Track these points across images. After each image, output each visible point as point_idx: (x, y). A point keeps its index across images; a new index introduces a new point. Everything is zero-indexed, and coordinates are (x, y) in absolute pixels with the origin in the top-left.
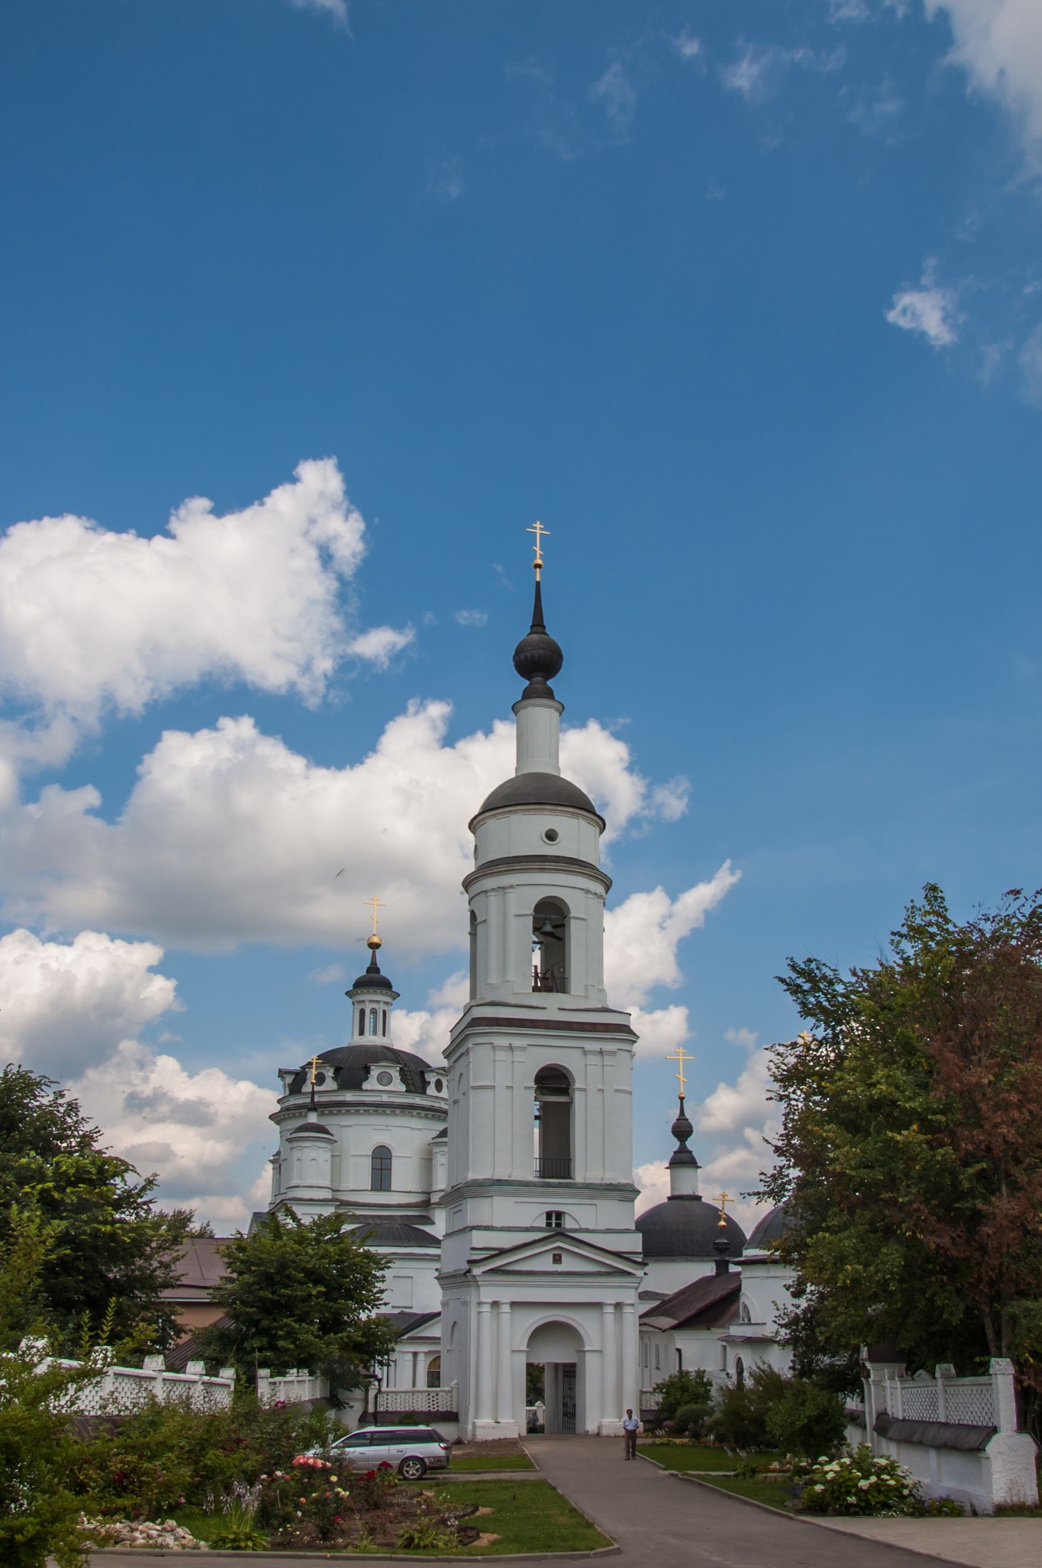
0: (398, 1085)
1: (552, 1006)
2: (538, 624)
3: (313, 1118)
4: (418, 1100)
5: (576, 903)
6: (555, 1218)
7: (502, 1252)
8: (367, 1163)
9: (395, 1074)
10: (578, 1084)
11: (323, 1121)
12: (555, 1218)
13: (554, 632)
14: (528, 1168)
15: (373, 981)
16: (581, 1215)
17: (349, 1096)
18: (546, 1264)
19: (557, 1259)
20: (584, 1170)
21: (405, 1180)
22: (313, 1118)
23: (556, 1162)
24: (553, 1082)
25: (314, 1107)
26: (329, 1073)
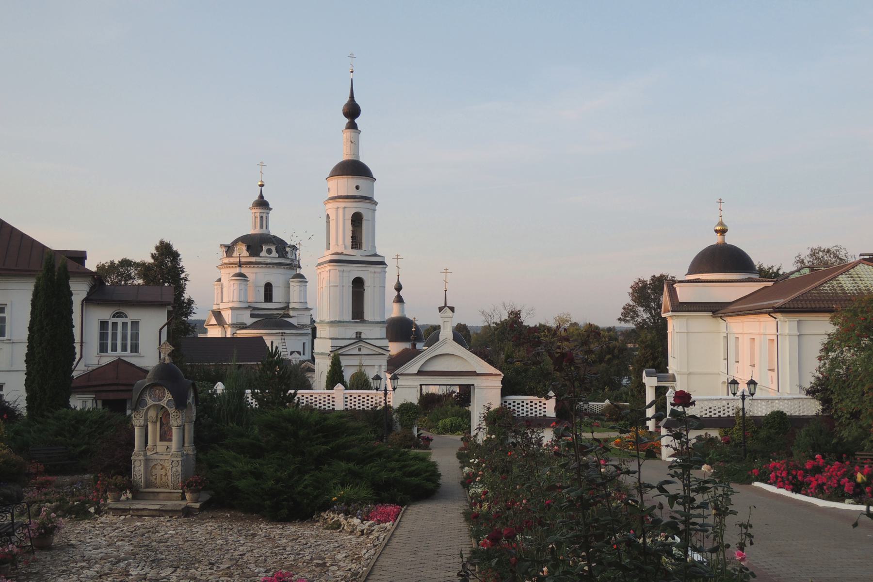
0: (274, 254)
1: (357, 255)
2: (352, 96)
3: (237, 270)
4: (283, 261)
5: (366, 216)
6: (359, 334)
7: (342, 347)
8: (263, 289)
9: (273, 248)
10: (366, 284)
11: (244, 270)
12: (359, 334)
13: (357, 100)
14: (348, 316)
15: (262, 204)
16: (368, 332)
17: (253, 259)
18: (356, 352)
19: (360, 350)
20: (368, 316)
21: (278, 295)
22: (237, 270)
23: (358, 313)
24: (358, 284)
25: (240, 265)
26: (244, 248)
